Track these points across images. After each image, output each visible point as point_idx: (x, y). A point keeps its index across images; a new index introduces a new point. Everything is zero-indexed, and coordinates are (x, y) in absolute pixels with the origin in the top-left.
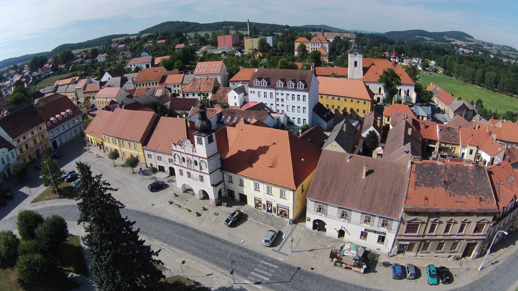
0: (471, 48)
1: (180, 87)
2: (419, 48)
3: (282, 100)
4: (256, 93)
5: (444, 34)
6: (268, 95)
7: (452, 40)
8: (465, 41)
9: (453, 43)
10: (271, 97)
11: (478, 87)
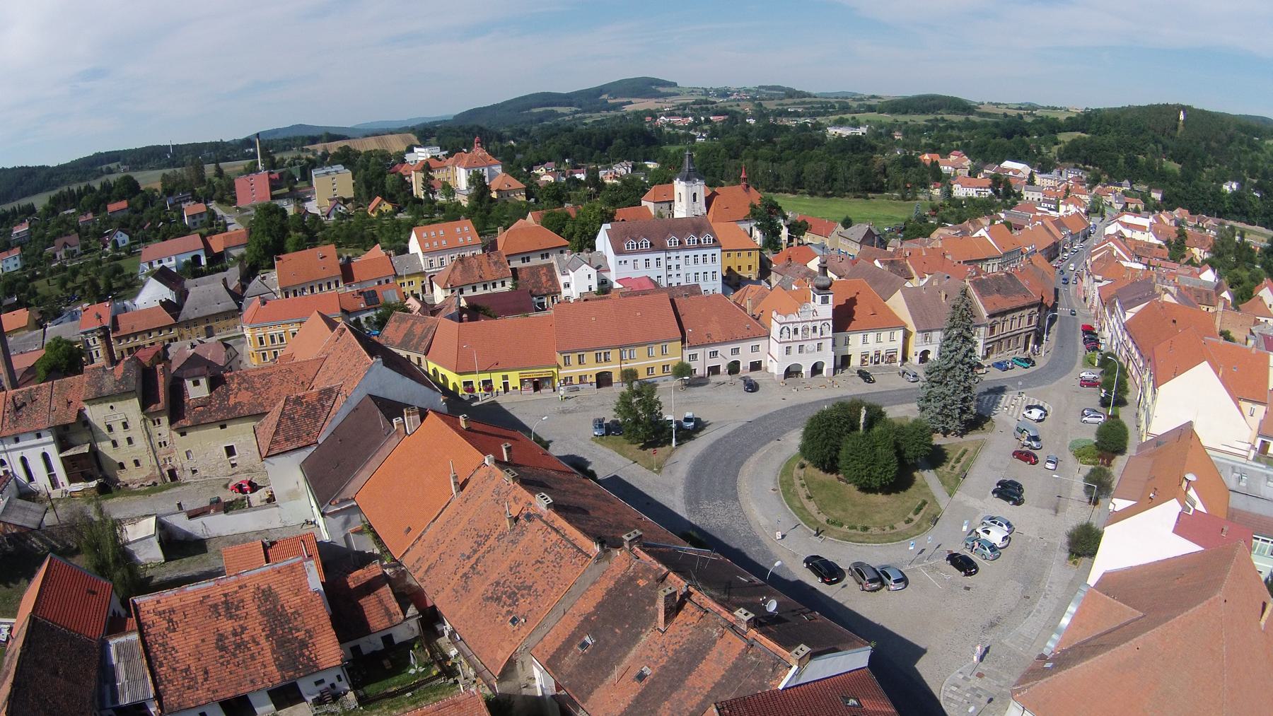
0: (687, 111)
2: (590, 139)
3: (678, 267)
4: (630, 262)
5: (600, 91)
6: (653, 262)
7: (625, 100)
9: (628, 108)
10: (658, 264)
11: (791, 196)
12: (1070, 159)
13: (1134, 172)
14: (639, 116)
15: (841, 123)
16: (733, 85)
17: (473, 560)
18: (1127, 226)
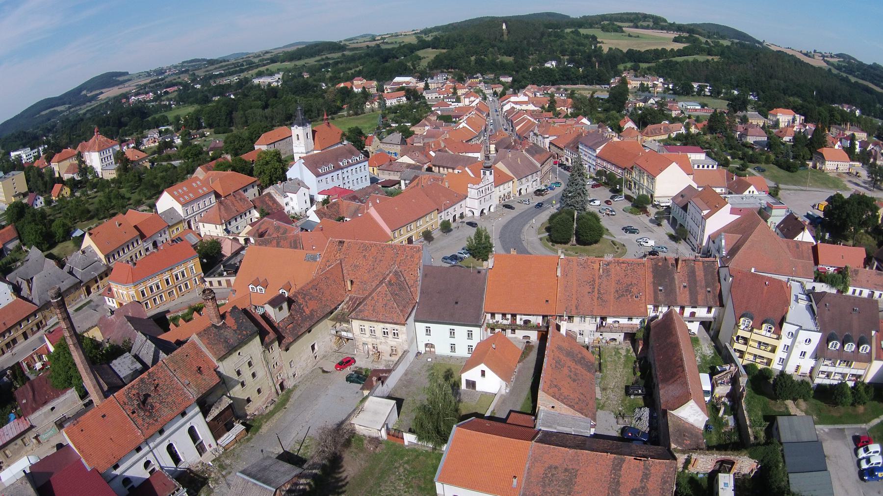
0: (147, 90)
1: (167, 232)
4: (324, 180)
7: (98, 92)
8: (117, 85)
12: (436, 68)
13: (482, 67)
14: (117, 99)
15: (260, 75)
16: (164, 65)
17: (596, 291)
18: (516, 103)
